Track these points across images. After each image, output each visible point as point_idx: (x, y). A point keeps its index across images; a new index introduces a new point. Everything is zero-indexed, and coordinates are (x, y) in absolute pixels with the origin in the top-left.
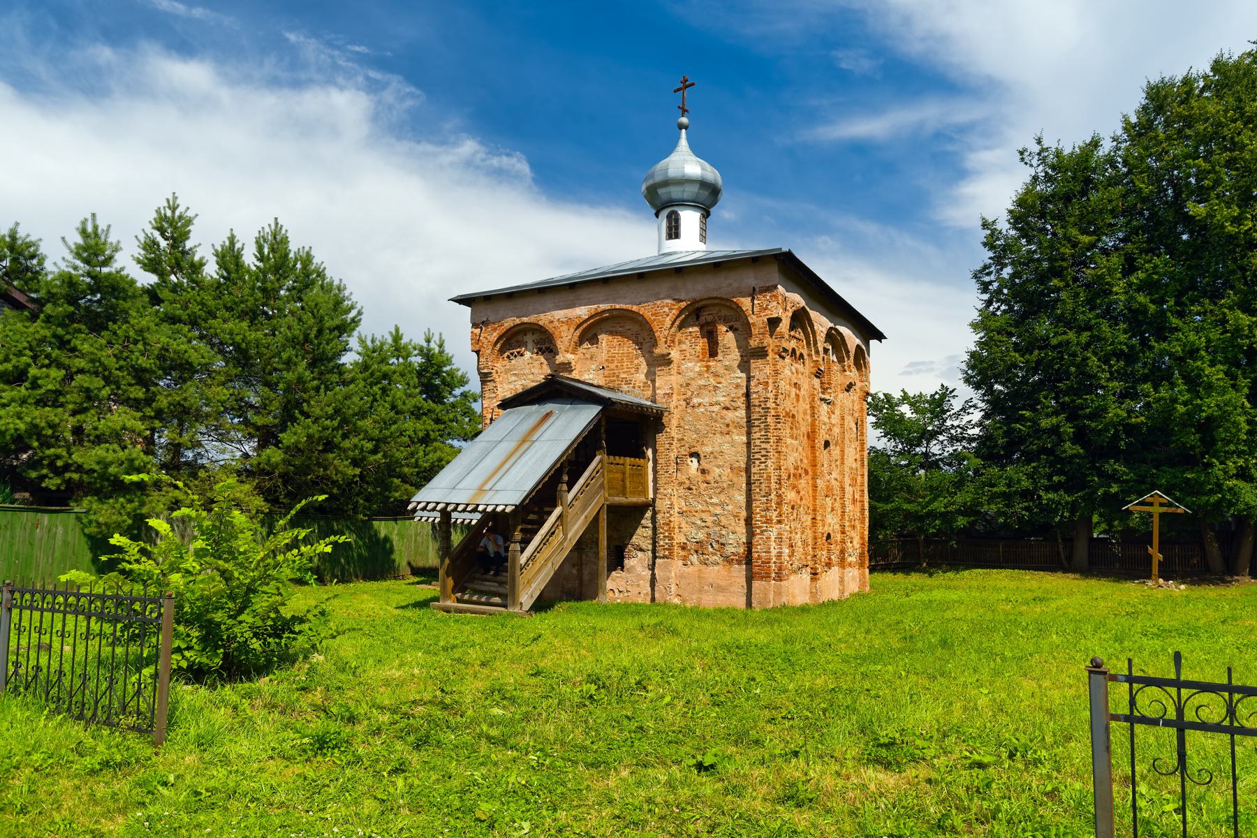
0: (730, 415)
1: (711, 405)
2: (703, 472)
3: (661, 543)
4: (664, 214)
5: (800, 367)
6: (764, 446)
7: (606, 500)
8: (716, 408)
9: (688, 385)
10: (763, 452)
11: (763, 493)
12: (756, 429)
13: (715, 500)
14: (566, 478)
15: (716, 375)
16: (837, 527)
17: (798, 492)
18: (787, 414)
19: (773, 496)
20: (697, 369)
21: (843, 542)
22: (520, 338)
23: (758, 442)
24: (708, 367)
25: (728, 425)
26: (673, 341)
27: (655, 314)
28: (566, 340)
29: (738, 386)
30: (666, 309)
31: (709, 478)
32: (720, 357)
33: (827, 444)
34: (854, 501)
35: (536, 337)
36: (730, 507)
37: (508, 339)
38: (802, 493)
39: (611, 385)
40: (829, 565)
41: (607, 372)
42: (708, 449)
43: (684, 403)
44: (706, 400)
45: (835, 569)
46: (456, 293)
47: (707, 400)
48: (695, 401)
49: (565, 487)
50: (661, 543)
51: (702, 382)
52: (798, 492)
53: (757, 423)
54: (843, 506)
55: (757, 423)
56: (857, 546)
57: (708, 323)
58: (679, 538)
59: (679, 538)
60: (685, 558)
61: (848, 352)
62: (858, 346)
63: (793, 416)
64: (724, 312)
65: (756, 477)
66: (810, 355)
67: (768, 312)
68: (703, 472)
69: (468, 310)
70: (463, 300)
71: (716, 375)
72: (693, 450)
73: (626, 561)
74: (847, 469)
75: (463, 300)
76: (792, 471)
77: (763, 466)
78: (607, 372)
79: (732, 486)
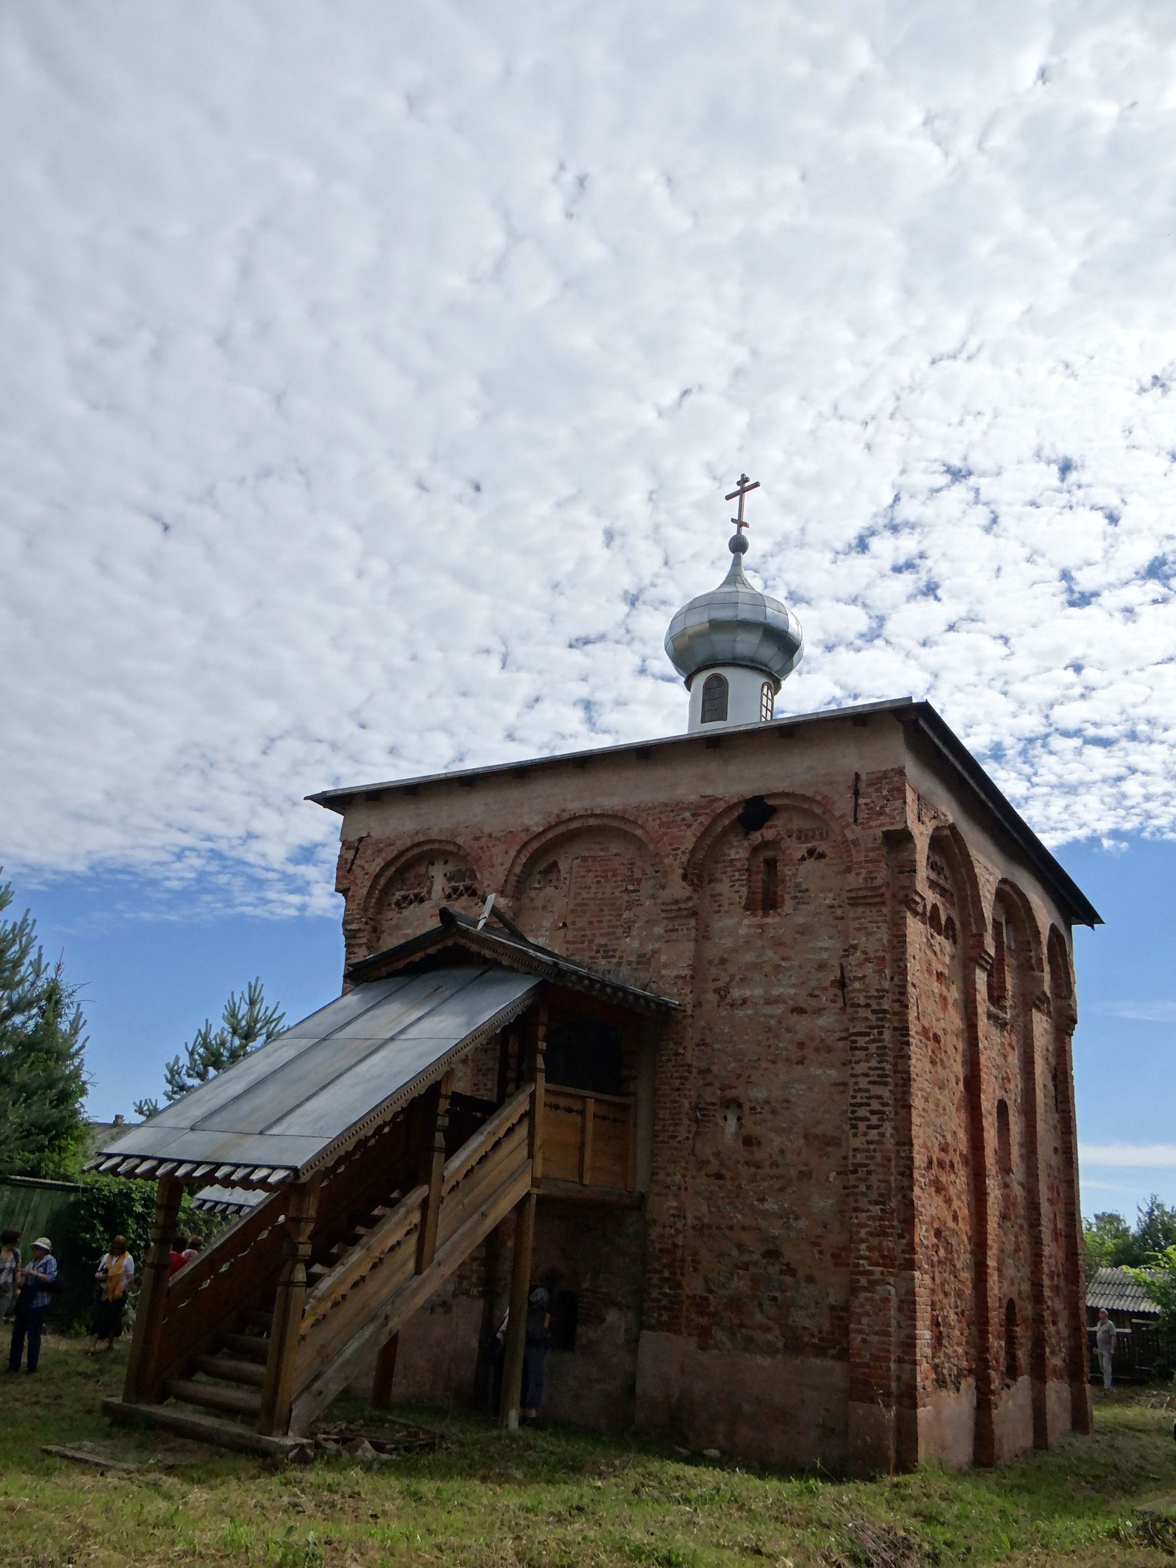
0: (804, 1025)
1: (769, 1002)
2: (748, 1142)
3: (655, 1294)
4: (700, 680)
5: (947, 944)
6: (876, 1090)
7: (535, 1182)
8: (778, 1010)
9: (723, 961)
10: (875, 1105)
11: (874, 1196)
12: (860, 1054)
13: (771, 1205)
14: (443, 1121)
15: (778, 943)
16: (1026, 1287)
17: (948, 1201)
18: (925, 1031)
19: (893, 1204)
20: (743, 931)
21: (1039, 1320)
22: (422, 870)
23: (863, 1083)
24: (761, 926)
25: (801, 1045)
26: (700, 877)
27: (668, 825)
28: (500, 873)
29: (821, 967)
30: (687, 814)
31: (759, 1155)
32: (788, 907)
33: (1002, 1107)
34: (1056, 1234)
35: (451, 868)
36: (803, 1223)
37: (401, 872)
38: (956, 1204)
39: (577, 958)
40: (1012, 1372)
41: (570, 935)
42: (759, 1093)
43: (713, 997)
44: (755, 992)
45: (1024, 1380)
46: (318, 789)
47: (759, 992)
48: (736, 993)
49: (440, 1139)
50: (655, 1294)
51: (749, 957)
52: (948, 1201)
53: (861, 1041)
54: (1037, 1242)
55: (861, 1041)
56: (1065, 1333)
57: (765, 845)
58: (694, 1286)
59: (694, 1286)
60: (704, 1334)
61: (1038, 933)
62: (1053, 928)
63: (936, 1039)
64: (798, 823)
65: (860, 1158)
66: (965, 924)
67: (883, 819)
68: (748, 1142)
69: (338, 819)
70: (329, 800)
71: (778, 943)
72: (730, 1093)
73: (580, 1330)
74: (1041, 1165)
75: (329, 800)
76: (936, 1155)
77: (873, 1134)
78: (570, 935)
79: (805, 1175)
